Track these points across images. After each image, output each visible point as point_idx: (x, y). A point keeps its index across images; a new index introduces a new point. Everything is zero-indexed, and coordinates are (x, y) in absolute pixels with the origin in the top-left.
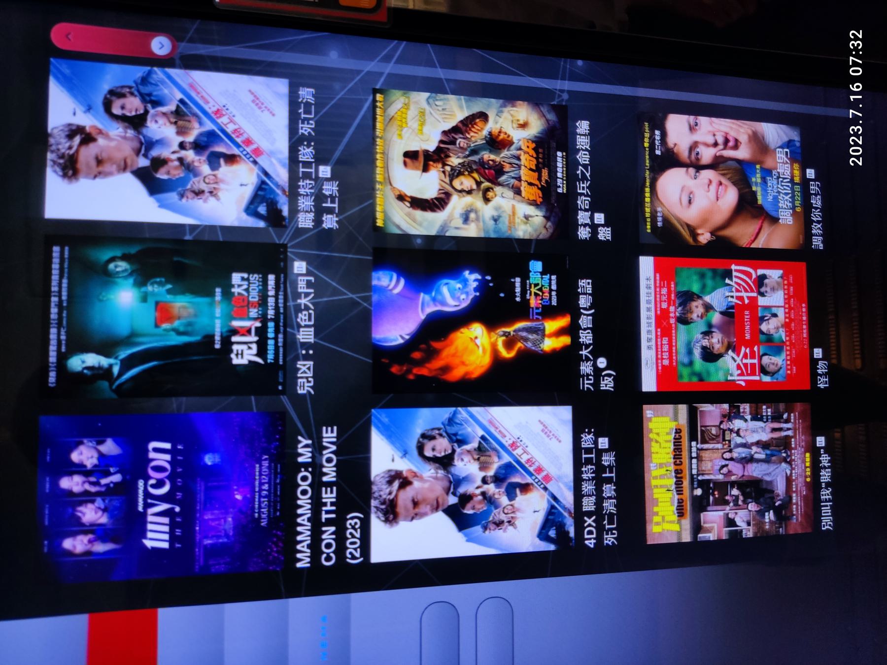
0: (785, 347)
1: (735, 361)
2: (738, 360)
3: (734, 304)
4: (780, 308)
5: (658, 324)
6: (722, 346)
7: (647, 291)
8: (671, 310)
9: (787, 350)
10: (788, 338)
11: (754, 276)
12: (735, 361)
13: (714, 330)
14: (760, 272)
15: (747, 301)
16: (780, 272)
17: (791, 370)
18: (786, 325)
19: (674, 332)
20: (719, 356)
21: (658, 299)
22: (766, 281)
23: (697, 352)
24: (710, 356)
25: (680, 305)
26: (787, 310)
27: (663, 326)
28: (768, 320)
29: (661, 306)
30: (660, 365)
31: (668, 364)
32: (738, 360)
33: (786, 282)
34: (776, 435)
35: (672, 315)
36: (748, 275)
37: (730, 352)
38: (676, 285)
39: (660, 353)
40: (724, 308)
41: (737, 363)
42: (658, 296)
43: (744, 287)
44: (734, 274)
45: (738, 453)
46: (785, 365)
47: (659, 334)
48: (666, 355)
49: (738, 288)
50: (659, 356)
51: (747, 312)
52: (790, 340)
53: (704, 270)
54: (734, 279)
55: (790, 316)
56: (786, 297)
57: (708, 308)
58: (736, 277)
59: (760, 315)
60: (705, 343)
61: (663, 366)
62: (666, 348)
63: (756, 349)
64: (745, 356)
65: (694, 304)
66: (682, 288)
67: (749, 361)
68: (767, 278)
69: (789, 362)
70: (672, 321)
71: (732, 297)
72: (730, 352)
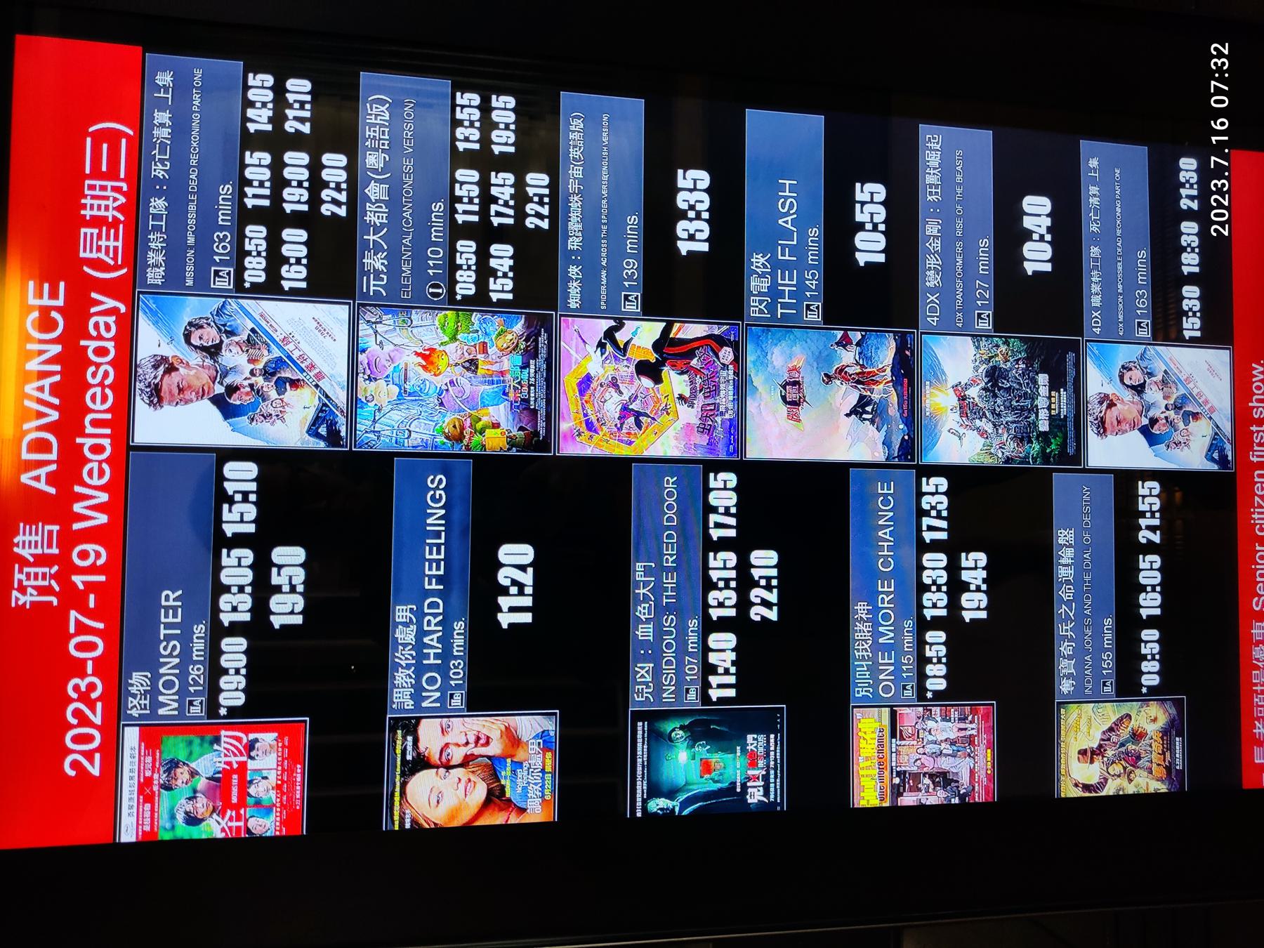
0: (274, 808)
1: (219, 823)
2: (223, 823)
3: (221, 769)
4: (272, 771)
5: (141, 790)
6: (207, 811)
7: (130, 760)
8: (154, 778)
9: (276, 812)
10: (278, 800)
11: (245, 741)
12: (219, 823)
13: (197, 795)
14: (252, 736)
15: (235, 766)
16: (275, 735)
17: (281, 831)
18: (278, 787)
19: (157, 798)
20: (202, 820)
21: (142, 768)
22: (257, 745)
23: (180, 817)
24: (192, 820)
25: (164, 772)
26: (279, 773)
27: (145, 793)
28: (257, 783)
29: (144, 774)
30: (140, 830)
31: (149, 830)
32: (223, 823)
33: (280, 744)
34: (963, 734)
35: (156, 782)
36: (239, 739)
37: (215, 816)
38: (160, 753)
39: (141, 819)
40: (210, 775)
41: (221, 827)
42: (142, 765)
43: (233, 752)
44: (223, 739)
45: (931, 748)
46: (274, 826)
47: (141, 801)
48: (147, 821)
49: (226, 752)
50: (140, 822)
51: (235, 776)
52: (281, 802)
53: (192, 737)
54: (223, 745)
55: (282, 778)
56: (280, 759)
57: (194, 773)
58: (225, 742)
59: (249, 779)
60: (189, 807)
61: (143, 832)
62: (147, 814)
63: (242, 811)
64: (231, 819)
65: (179, 771)
66: (167, 756)
67: (234, 824)
68: (259, 741)
69: (278, 824)
70: (155, 788)
71: (220, 762)
72: (215, 816)
